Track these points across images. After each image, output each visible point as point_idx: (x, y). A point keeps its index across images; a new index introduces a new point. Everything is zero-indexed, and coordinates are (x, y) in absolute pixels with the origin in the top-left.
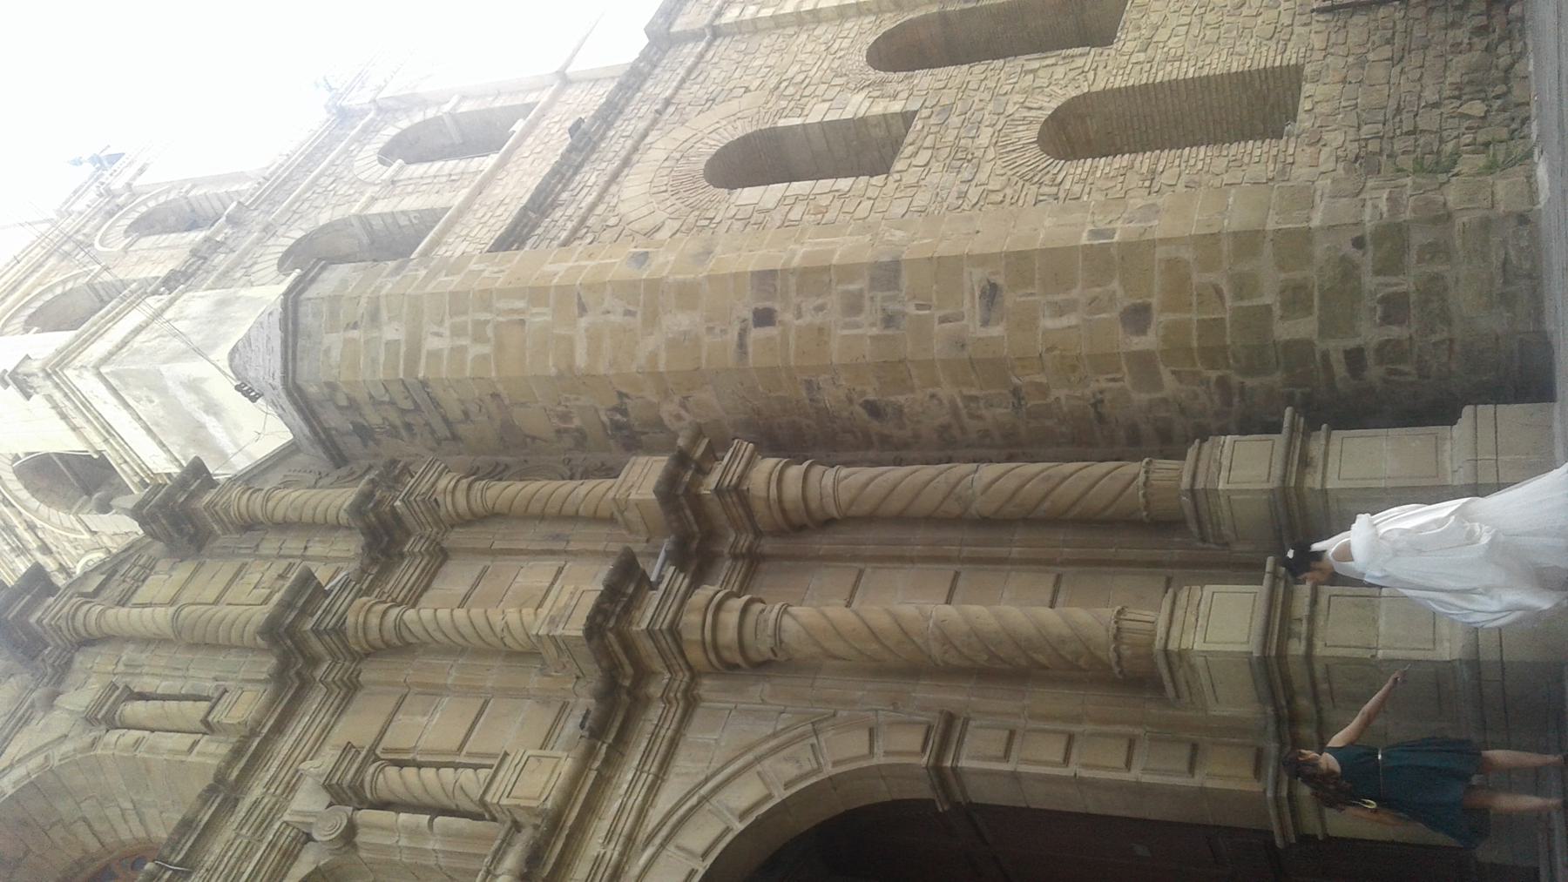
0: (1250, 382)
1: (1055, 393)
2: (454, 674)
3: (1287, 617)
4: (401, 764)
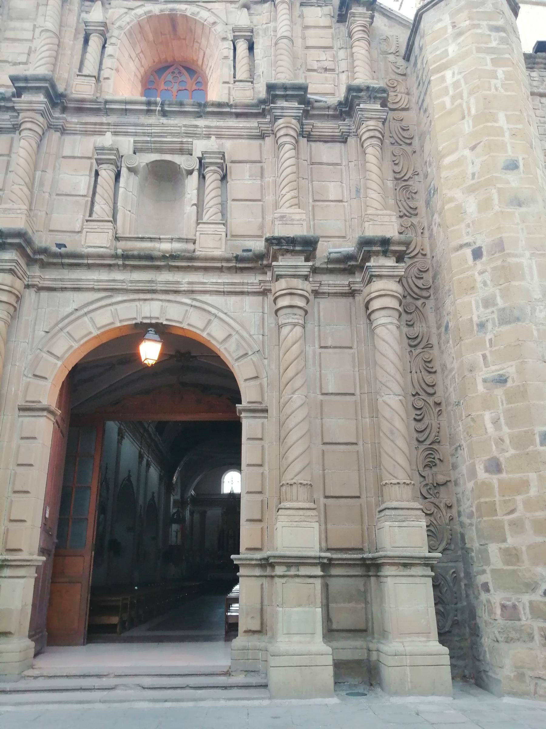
0: (474, 528)
1: (460, 423)
2: (271, 180)
3: (298, 565)
4: (224, 178)
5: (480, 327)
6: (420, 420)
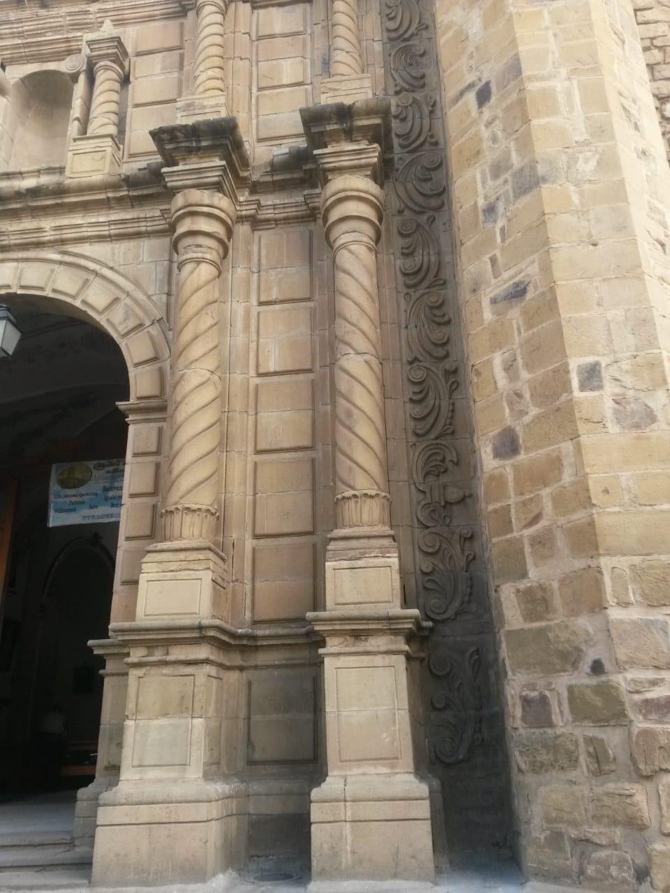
3: (168, 643)
5: (487, 214)
6: (420, 402)
